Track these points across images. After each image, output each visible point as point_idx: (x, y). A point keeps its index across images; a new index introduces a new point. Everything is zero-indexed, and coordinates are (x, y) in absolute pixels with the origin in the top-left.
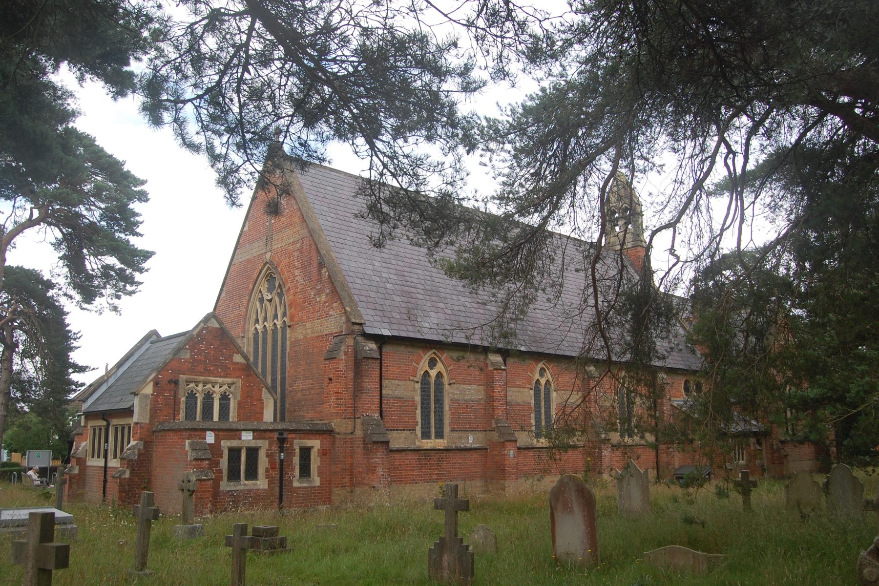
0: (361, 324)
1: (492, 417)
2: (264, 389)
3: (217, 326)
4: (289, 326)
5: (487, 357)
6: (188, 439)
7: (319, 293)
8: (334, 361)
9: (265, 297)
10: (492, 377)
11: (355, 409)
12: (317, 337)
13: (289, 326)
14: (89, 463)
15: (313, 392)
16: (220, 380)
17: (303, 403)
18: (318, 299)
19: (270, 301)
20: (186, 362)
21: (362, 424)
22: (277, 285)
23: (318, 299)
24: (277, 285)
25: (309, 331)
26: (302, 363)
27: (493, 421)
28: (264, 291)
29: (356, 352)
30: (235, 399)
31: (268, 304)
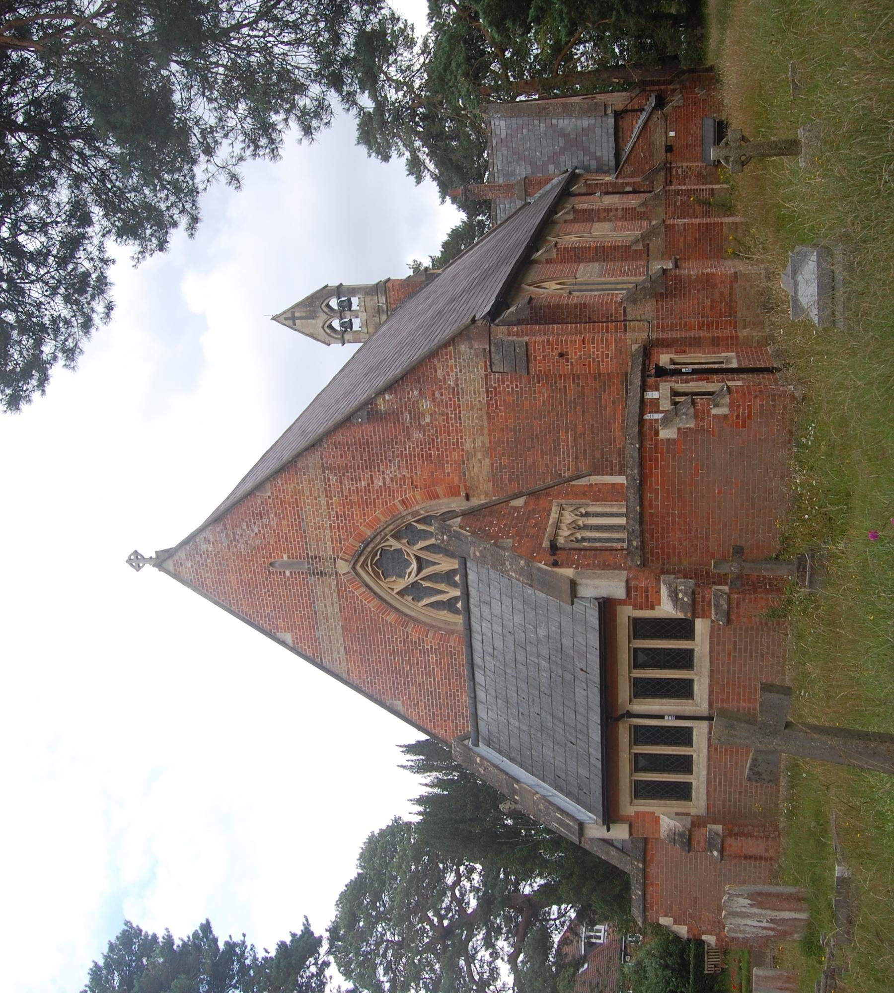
0: (474, 320)
1: (627, 248)
2: (573, 483)
3: (459, 519)
4: (467, 498)
5: (535, 262)
6: (657, 433)
7: (417, 416)
8: (531, 348)
9: (412, 579)
10: (568, 250)
11: (610, 319)
12: (489, 418)
13: (467, 498)
14: (702, 811)
15: (580, 428)
16: (554, 515)
17: (598, 455)
18: (428, 420)
19: (422, 563)
20: (519, 542)
21: (635, 302)
22: (395, 544)
23: (428, 420)
24: (395, 544)
25: (478, 443)
26: (530, 460)
27: (634, 248)
28: (401, 584)
29: (519, 323)
30: (588, 505)
31: (425, 572)
